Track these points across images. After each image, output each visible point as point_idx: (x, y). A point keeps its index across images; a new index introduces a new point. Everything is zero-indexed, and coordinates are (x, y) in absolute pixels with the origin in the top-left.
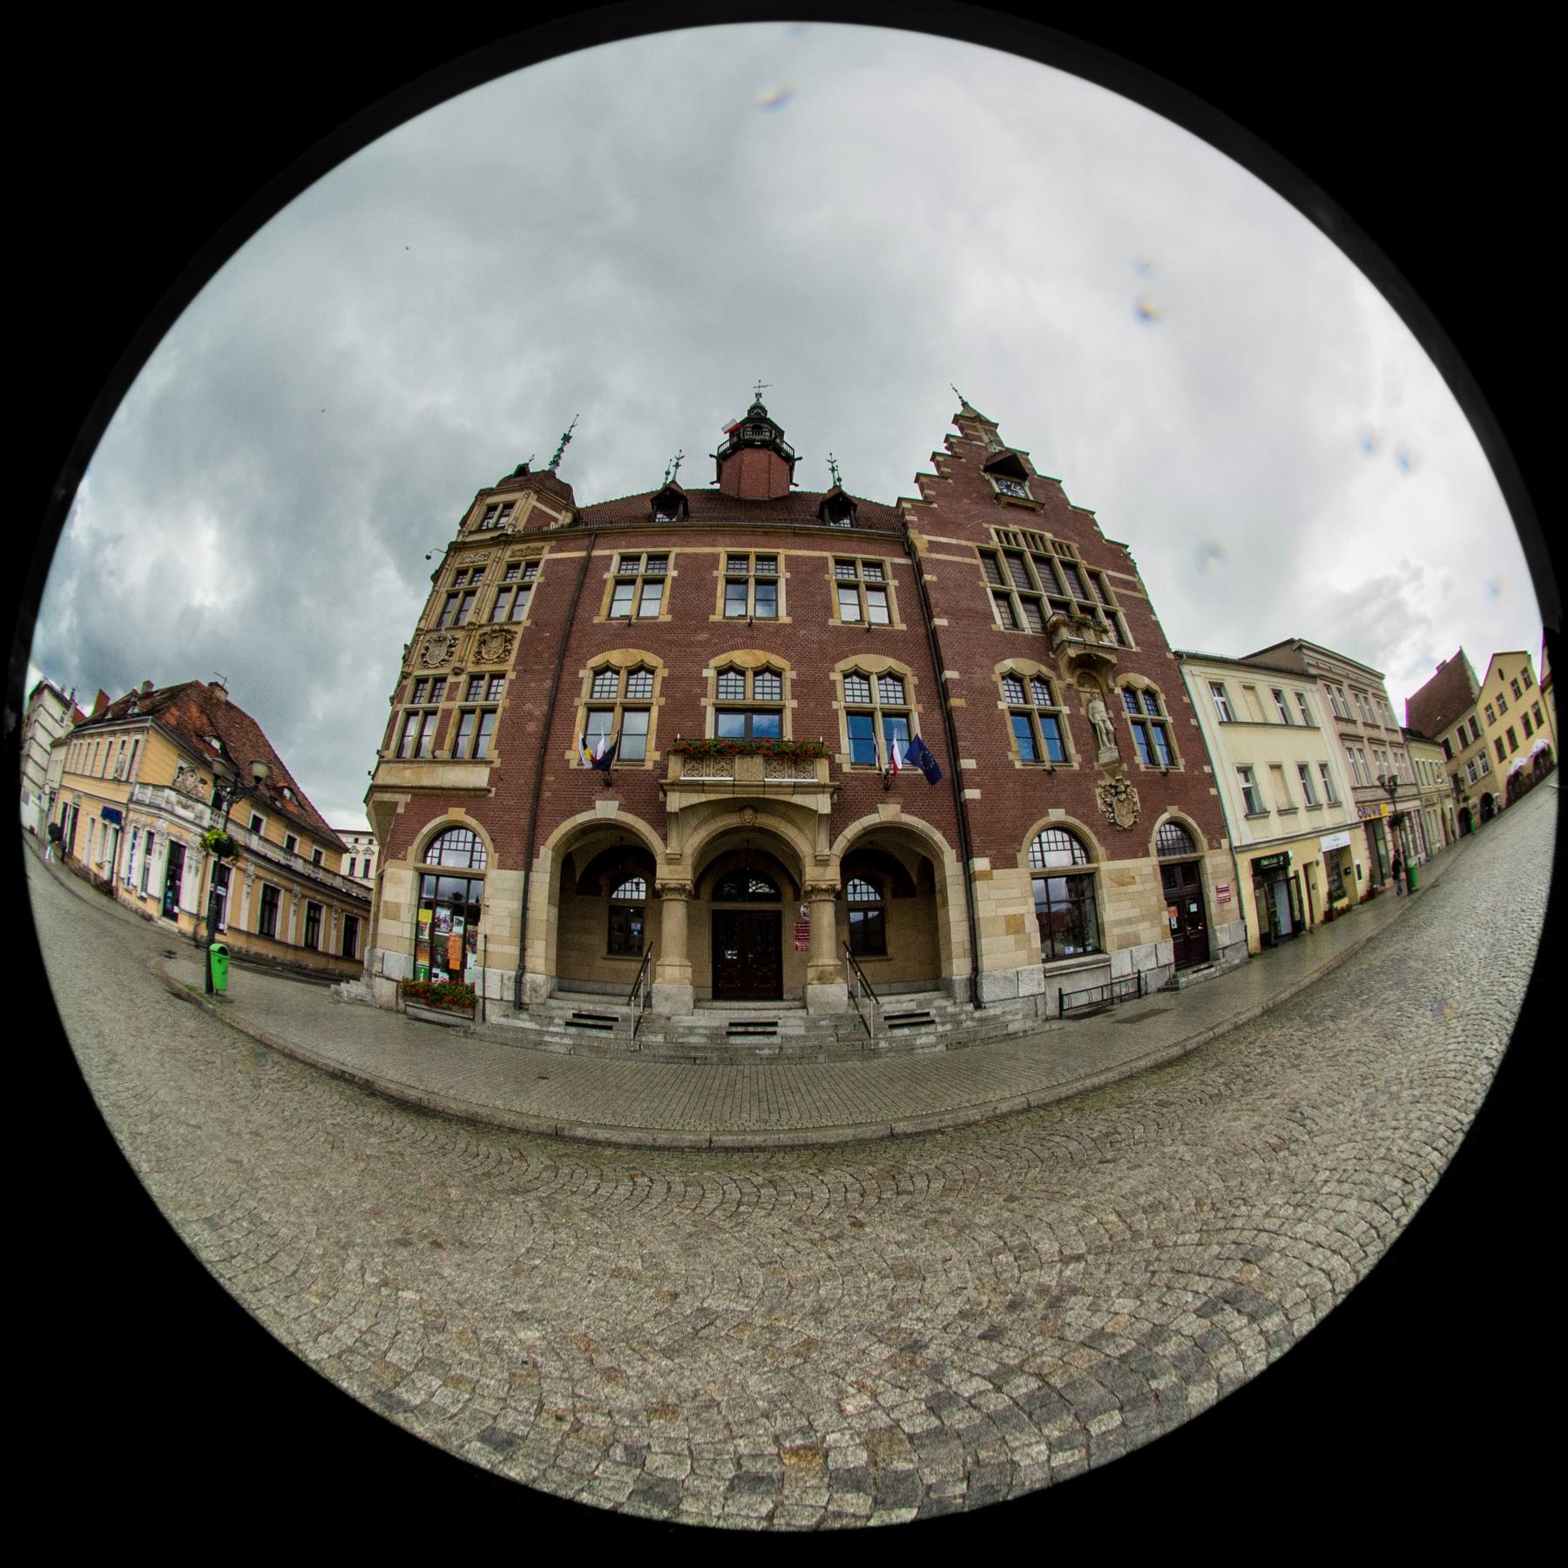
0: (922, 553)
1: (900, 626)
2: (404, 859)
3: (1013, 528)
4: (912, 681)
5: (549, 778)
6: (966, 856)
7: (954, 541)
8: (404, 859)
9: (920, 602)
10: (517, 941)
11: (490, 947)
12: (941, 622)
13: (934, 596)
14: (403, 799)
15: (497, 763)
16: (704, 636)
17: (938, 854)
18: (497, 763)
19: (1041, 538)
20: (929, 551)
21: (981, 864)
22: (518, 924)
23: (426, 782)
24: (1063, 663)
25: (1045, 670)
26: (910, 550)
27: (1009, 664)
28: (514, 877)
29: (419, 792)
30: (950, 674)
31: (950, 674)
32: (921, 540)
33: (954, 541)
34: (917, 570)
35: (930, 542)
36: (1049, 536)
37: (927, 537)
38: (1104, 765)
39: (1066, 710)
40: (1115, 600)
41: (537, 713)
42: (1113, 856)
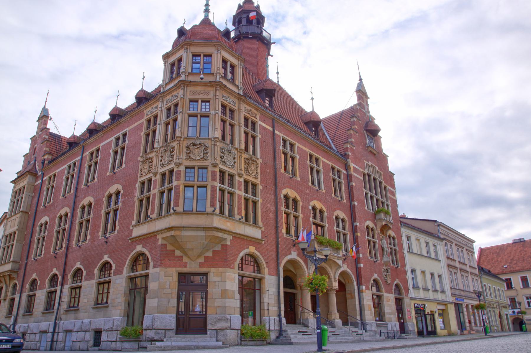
1: (345, 201)
2: (233, 268)
4: (347, 223)
5: (280, 240)
6: (359, 284)
8: (233, 268)
10: (277, 305)
11: (270, 308)
14: (229, 238)
15: (263, 229)
16: (308, 192)
17: (352, 282)
18: (263, 229)
21: (364, 287)
22: (276, 298)
23: (238, 231)
26: (347, 168)
28: (273, 278)
29: (237, 236)
30: (358, 224)
32: (352, 165)
34: (349, 178)
36: (377, 168)
38: (384, 262)
42: (386, 292)
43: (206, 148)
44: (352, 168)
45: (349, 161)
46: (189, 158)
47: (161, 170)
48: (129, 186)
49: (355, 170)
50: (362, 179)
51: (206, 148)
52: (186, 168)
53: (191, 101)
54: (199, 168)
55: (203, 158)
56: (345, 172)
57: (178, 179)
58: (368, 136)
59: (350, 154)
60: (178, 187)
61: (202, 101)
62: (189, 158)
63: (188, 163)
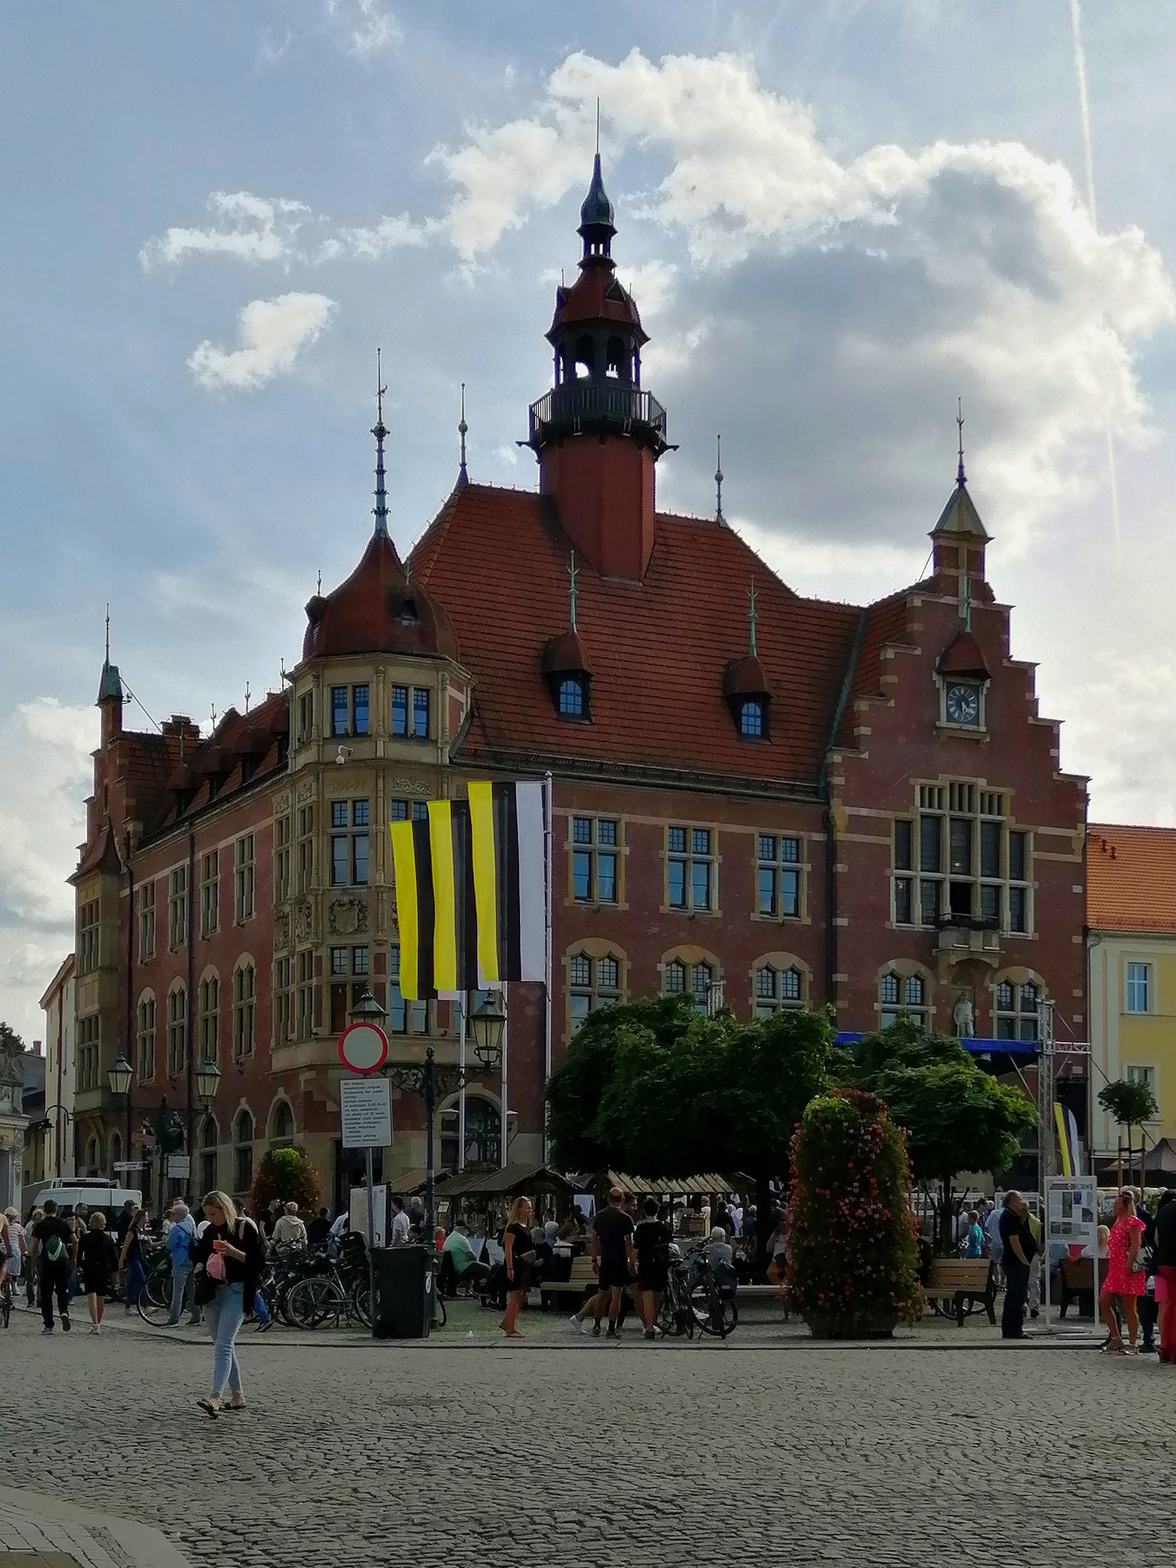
0: (840, 836)
1: (806, 920)
3: (943, 780)
4: (808, 977)
7: (873, 813)
9: (828, 897)
12: (841, 922)
13: (841, 889)
16: (655, 930)
19: (970, 787)
20: (849, 830)
24: (942, 967)
25: (923, 969)
26: (827, 825)
27: (892, 964)
30: (840, 977)
31: (840, 977)
32: (841, 812)
33: (873, 813)
34: (830, 852)
35: (852, 817)
36: (982, 783)
37: (849, 810)
39: (933, 1010)
40: (1030, 871)
41: (532, 998)
43: (363, 909)
44: (840, 821)
45: (836, 802)
46: (334, 931)
47: (300, 948)
48: (263, 959)
49: (855, 823)
50: (891, 841)
51: (363, 909)
52: (333, 949)
53: (333, 803)
54: (354, 948)
55: (359, 930)
56: (818, 837)
57: (319, 974)
58: (950, 687)
59: (838, 780)
60: (319, 988)
61: (354, 802)
62: (334, 931)
63: (333, 941)
